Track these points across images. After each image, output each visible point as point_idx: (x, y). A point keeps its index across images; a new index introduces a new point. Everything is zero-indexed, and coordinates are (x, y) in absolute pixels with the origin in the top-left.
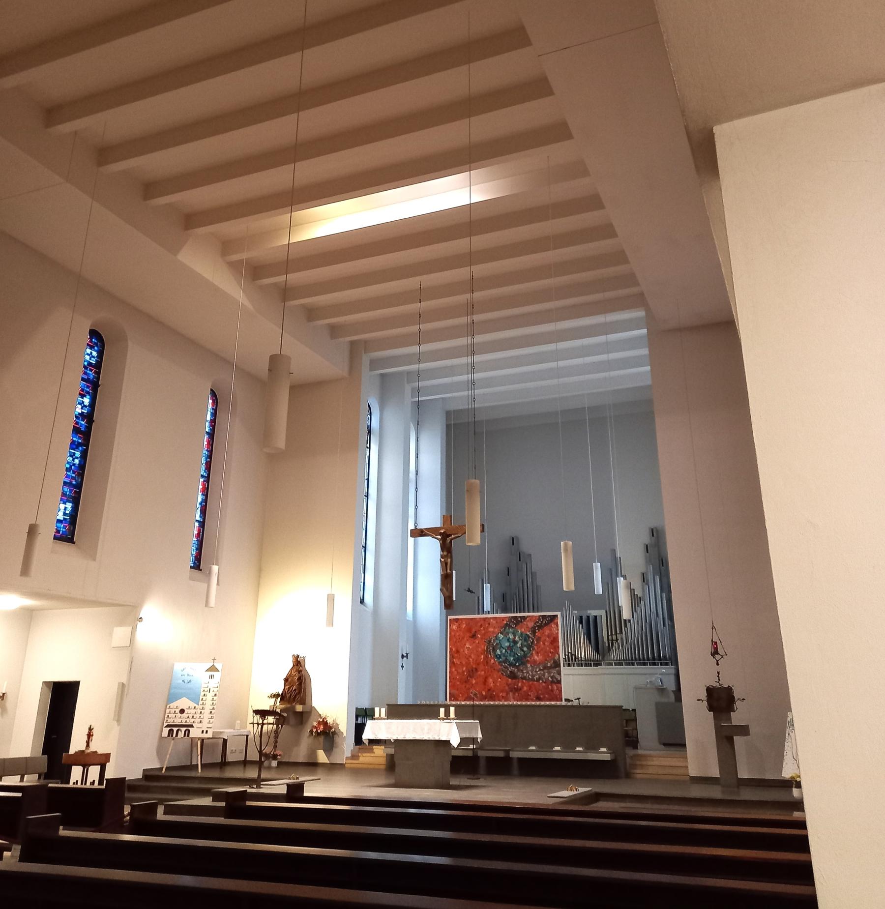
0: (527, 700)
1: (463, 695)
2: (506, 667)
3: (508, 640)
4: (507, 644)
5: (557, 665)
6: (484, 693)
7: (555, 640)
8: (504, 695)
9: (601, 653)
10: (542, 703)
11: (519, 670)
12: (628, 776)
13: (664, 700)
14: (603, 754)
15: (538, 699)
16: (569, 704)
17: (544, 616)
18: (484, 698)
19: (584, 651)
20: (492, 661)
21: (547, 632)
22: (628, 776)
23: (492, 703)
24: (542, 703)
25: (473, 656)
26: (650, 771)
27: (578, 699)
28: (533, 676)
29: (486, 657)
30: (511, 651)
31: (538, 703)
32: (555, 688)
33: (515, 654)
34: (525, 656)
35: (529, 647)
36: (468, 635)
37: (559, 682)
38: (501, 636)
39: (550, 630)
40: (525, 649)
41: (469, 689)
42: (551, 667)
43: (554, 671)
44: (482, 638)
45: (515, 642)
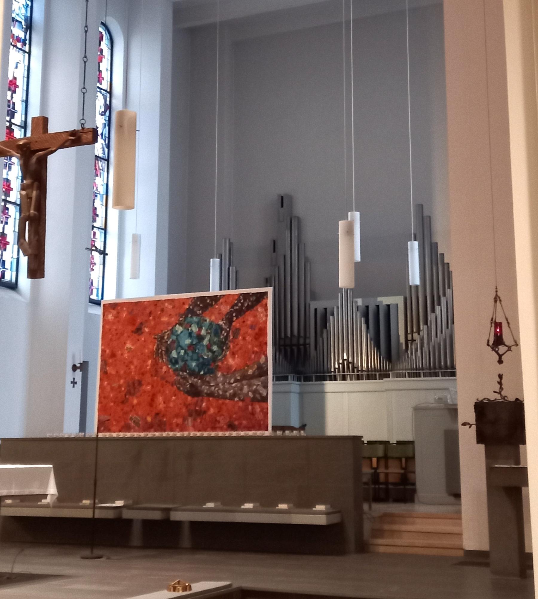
0: (214, 429)
1: (118, 422)
2: (184, 378)
3: (190, 335)
4: (188, 341)
5: (262, 372)
6: (149, 419)
7: (262, 332)
8: (180, 421)
9: (389, 358)
10: (234, 434)
11: (204, 382)
12: (363, 548)
14: (318, 515)
15: (231, 427)
17: (246, 296)
18: (149, 427)
20: (164, 369)
21: (250, 320)
22: (363, 548)
23: (157, 434)
24: (234, 434)
25: (135, 362)
26: (405, 540)
28: (225, 391)
29: (155, 364)
30: (194, 351)
31: (227, 434)
32: (258, 408)
33: (200, 357)
34: (214, 359)
35: (222, 345)
36: (130, 328)
37: (265, 399)
38: (179, 329)
39: (255, 316)
40: (215, 348)
41: (126, 413)
42: (253, 377)
43: (257, 383)
44: (150, 333)
45: (201, 338)
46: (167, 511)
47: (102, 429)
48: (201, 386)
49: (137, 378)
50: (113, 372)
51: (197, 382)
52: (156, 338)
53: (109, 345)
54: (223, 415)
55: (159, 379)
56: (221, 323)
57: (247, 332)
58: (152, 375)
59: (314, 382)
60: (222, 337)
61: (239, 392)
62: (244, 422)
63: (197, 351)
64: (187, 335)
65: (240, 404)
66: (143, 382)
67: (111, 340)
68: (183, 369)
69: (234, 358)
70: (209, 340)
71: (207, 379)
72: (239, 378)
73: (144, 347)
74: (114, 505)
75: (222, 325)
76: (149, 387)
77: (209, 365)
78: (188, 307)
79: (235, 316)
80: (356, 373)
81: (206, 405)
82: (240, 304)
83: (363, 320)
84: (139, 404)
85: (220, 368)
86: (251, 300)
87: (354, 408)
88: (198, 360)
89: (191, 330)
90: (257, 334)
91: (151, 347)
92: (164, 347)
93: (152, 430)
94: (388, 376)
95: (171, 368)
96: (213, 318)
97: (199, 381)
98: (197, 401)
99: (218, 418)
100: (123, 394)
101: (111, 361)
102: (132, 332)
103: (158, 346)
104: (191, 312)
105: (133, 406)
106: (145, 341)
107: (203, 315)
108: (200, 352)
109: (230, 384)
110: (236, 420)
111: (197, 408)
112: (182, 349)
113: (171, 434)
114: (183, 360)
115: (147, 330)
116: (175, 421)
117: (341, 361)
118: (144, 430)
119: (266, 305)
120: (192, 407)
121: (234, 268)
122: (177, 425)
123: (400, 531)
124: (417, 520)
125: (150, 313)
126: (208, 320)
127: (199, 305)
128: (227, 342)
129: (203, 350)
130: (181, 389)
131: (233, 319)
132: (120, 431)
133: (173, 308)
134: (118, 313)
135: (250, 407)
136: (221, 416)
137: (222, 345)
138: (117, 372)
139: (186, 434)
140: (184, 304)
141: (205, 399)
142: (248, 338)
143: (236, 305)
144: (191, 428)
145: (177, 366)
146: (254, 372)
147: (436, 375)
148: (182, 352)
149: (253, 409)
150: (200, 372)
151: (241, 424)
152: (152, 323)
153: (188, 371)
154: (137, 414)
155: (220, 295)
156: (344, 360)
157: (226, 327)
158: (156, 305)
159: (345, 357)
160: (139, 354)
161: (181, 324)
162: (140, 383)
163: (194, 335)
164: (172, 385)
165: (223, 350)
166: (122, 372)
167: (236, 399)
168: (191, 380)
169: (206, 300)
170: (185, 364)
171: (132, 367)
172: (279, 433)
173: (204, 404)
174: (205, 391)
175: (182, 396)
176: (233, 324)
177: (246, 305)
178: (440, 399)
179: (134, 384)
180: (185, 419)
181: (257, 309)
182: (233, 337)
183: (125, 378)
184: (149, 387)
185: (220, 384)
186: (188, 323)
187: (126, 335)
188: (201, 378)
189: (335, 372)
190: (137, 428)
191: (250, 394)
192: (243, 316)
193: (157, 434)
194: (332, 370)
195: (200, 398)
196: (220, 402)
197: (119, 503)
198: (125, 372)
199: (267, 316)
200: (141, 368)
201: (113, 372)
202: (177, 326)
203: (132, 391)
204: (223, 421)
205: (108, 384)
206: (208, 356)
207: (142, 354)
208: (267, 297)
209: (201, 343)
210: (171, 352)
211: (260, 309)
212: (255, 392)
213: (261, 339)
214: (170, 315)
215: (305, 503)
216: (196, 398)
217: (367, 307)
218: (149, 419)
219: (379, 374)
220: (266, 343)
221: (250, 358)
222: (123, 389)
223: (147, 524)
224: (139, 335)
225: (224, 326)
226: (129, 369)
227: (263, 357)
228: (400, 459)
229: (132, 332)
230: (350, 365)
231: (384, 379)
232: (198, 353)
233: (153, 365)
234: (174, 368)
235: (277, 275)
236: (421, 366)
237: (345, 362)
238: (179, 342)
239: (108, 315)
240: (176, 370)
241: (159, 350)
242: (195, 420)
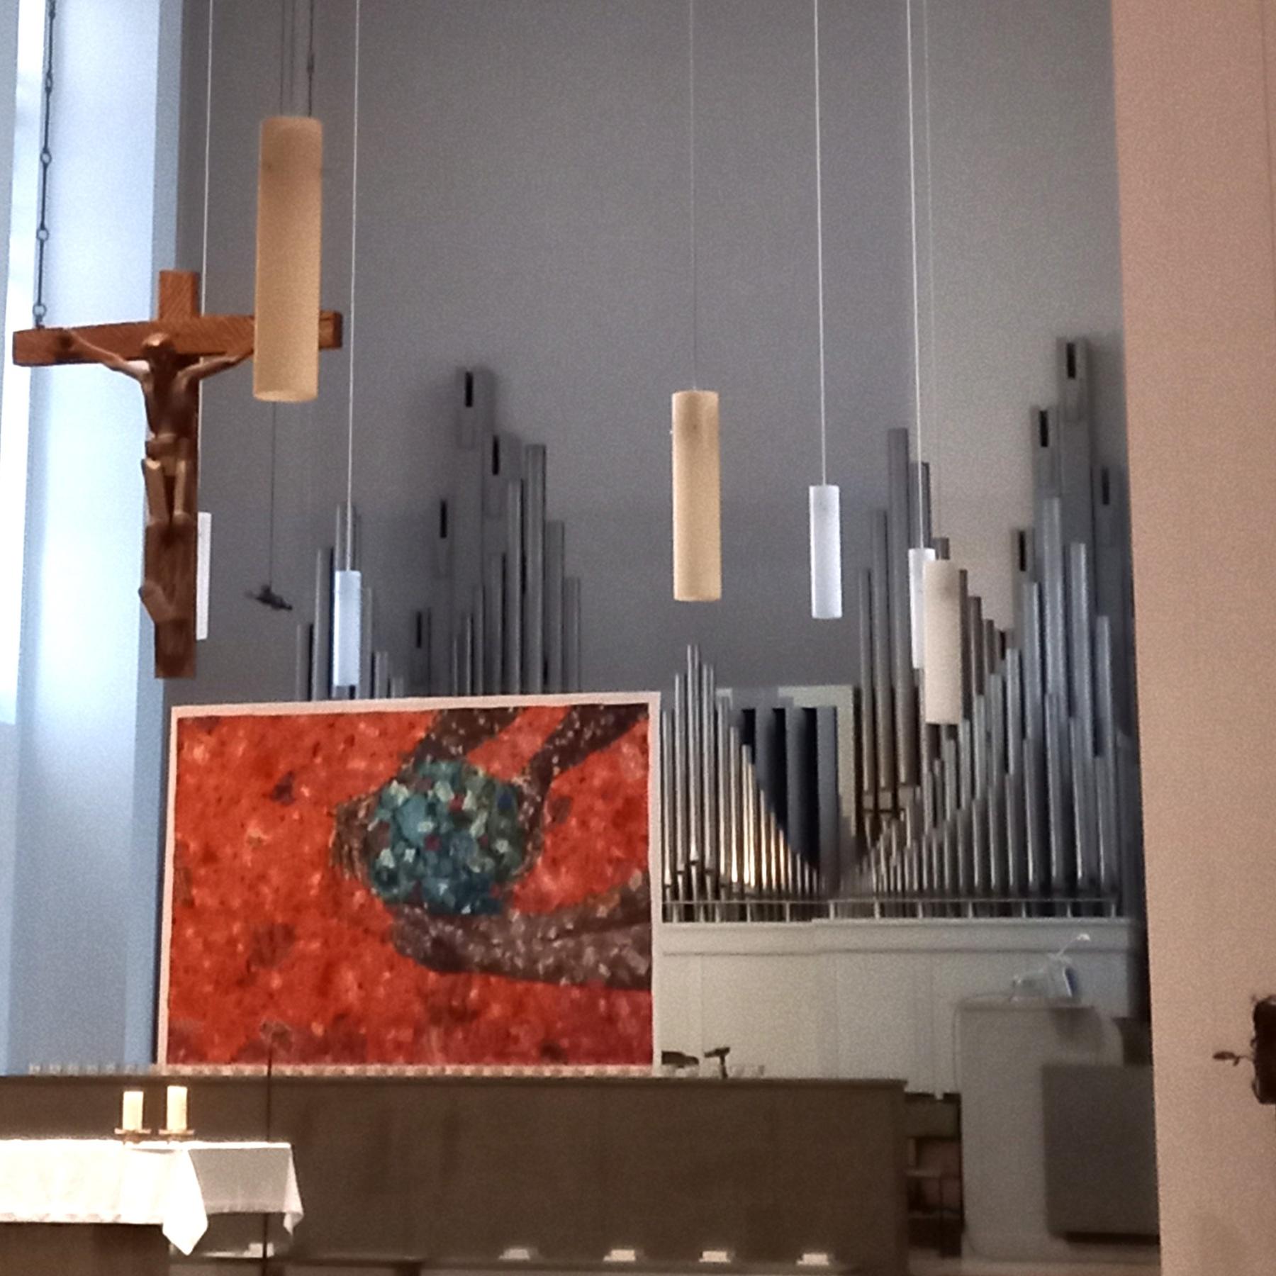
0: (502, 1056)
2: (417, 923)
3: (432, 809)
4: (426, 826)
5: (635, 912)
7: (634, 809)
11: (471, 933)
13: (1075, 1056)
15: (551, 1052)
16: (682, 1073)
17: (588, 712)
19: (754, 859)
20: (359, 896)
25: (275, 875)
27: (721, 1053)
28: (532, 960)
29: (333, 883)
30: (443, 853)
31: (548, 1071)
32: (623, 1006)
33: (458, 869)
34: (501, 874)
35: (523, 838)
36: (257, 785)
37: (644, 983)
38: (400, 793)
39: (614, 767)
40: (503, 846)
44: (316, 802)
45: (461, 819)
48: (465, 945)
49: (280, 919)
51: (453, 934)
54: (528, 1022)
55: (345, 925)
56: (518, 780)
57: (591, 809)
58: (323, 914)
60: (521, 818)
61: (573, 962)
62: (586, 1042)
63: (451, 853)
64: (423, 809)
65: (576, 993)
66: (299, 931)
67: (203, 815)
71: (483, 927)
72: (570, 926)
75: (520, 787)
76: (315, 946)
79: (559, 764)
81: (479, 995)
82: (570, 734)
85: (517, 898)
86: (603, 722)
87: (727, 997)
88: (454, 875)
89: (435, 796)
90: (618, 813)
92: (356, 840)
93: (328, 1058)
94: (822, 912)
95: (378, 895)
96: (496, 766)
97: (460, 932)
99: (514, 1031)
100: (241, 962)
101: (202, 872)
102: (264, 795)
103: (339, 835)
104: (432, 748)
105: (271, 996)
106: (301, 821)
107: (469, 757)
109: (546, 941)
111: (455, 1003)
112: (410, 846)
115: (306, 791)
116: (392, 1034)
117: (681, 867)
119: (644, 738)
122: (399, 1046)
125: (315, 750)
126: (481, 773)
128: (536, 831)
130: (409, 951)
131: (551, 772)
133: (380, 735)
134: (223, 743)
135: (602, 1003)
136: (522, 1023)
137: (523, 838)
138: (222, 903)
140: (412, 726)
142: (596, 824)
143: (561, 734)
144: (439, 1055)
145: (395, 891)
148: (410, 854)
149: (611, 1005)
150: (459, 907)
152: (323, 774)
153: (426, 906)
155: (516, 709)
156: (688, 864)
157: (534, 793)
158: (332, 726)
159: (694, 855)
160: (285, 855)
161: (402, 781)
162: (289, 934)
163: (443, 810)
164: (383, 941)
165: (524, 852)
166: (236, 903)
167: (563, 981)
168: (436, 927)
169: (476, 720)
170: (419, 884)
171: (266, 890)
173: (474, 994)
174: (477, 959)
175: (410, 970)
176: (553, 785)
177: (588, 734)
179: (271, 935)
180: (419, 1032)
181: (619, 748)
182: (554, 819)
183: (246, 920)
184: (315, 946)
185: (519, 943)
186: (424, 777)
187: (245, 802)
188: (465, 923)
191: (603, 969)
192: (580, 765)
195: (462, 977)
196: (520, 987)
198: (246, 904)
199: (646, 767)
200: (290, 895)
202: (395, 783)
204: (525, 1037)
205: (198, 934)
206: (483, 867)
207: (293, 856)
208: (647, 718)
209: (463, 832)
210: (378, 855)
211: (626, 749)
212: (615, 964)
213: (632, 827)
214: (373, 755)
216: (449, 979)
218: (318, 1029)
219: (792, 906)
220: (645, 839)
222: (240, 947)
224: (285, 804)
225: (526, 789)
226: (258, 894)
229: (264, 795)
230: (708, 880)
232: (454, 861)
233: (324, 888)
234: (386, 895)
236: (916, 886)
237: (694, 870)
238: (399, 829)
239: (191, 749)
240: (391, 903)
241: (342, 847)
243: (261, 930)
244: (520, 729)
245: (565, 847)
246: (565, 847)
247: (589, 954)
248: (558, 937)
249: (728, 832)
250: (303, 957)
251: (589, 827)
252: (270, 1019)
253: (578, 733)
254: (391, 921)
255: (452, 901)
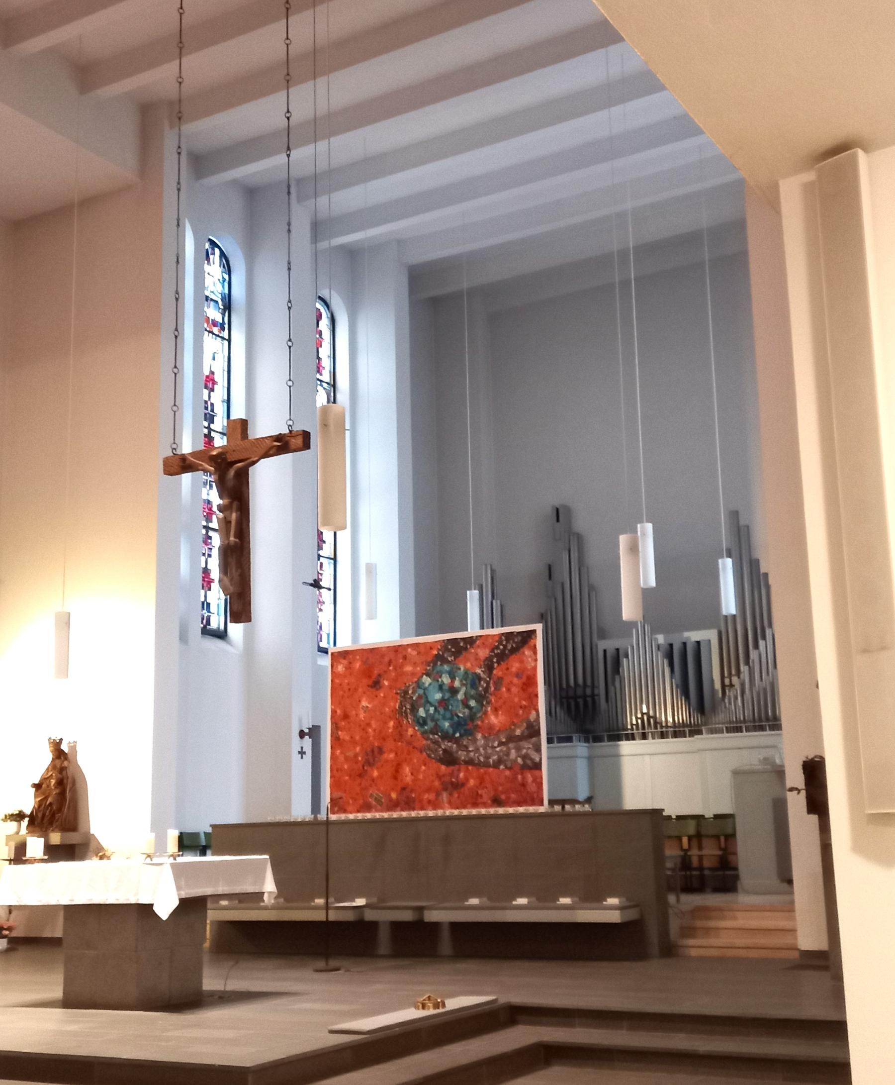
0: (475, 805)
1: (355, 799)
2: (436, 742)
3: (441, 688)
4: (438, 696)
5: (534, 732)
6: (394, 795)
7: (531, 682)
8: (432, 796)
9: (702, 708)
10: (501, 811)
12: (669, 950)
14: (610, 911)
15: (497, 802)
17: (509, 636)
18: (393, 806)
20: (410, 731)
22: (669, 950)
23: (404, 814)
24: (501, 811)
25: (373, 723)
26: (724, 940)
28: (487, 757)
29: (399, 725)
30: (446, 709)
31: (492, 811)
32: (529, 778)
33: (454, 714)
34: (472, 717)
35: (481, 698)
37: (538, 766)
38: (426, 680)
39: (522, 662)
40: (472, 703)
42: (522, 738)
43: (527, 747)
45: (454, 691)
46: (421, 909)
47: (336, 809)
48: (457, 752)
49: (376, 744)
50: (347, 738)
51: (451, 747)
52: (397, 693)
53: (340, 703)
56: (478, 671)
57: (511, 682)
58: (395, 740)
59: (606, 743)
62: (513, 796)
65: (508, 773)
66: (385, 749)
67: (343, 697)
68: (434, 731)
69: (497, 716)
70: (465, 694)
72: (504, 740)
73: (384, 704)
74: (354, 904)
76: (392, 756)
77: (466, 724)
78: (436, 652)
80: (659, 730)
82: (501, 647)
83: (666, 662)
84: (381, 776)
85: (480, 728)
88: (451, 719)
90: (524, 684)
91: (392, 704)
92: (409, 704)
93: (399, 808)
94: (700, 732)
96: (469, 665)
98: (453, 771)
99: (480, 792)
100: (360, 765)
103: (401, 702)
104: (440, 658)
105: (373, 780)
106: (384, 697)
108: (454, 708)
109: (493, 747)
110: (502, 793)
112: (432, 705)
113: (422, 813)
114: (433, 720)
115: (386, 683)
116: (426, 796)
117: (639, 716)
118: (388, 809)
119: (535, 646)
120: (447, 779)
121: (499, 602)
122: (429, 802)
123: (718, 929)
124: (738, 914)
125: (390, 663)
126: (462, 669)
127: (450, 650)
129: (457, 706)
132: (358, 811)
134: (350, 663)
135: (519, 777)
137: (481, 698)
139: (440, 812)
140: (431, 648)
141: (463, 767)
142: (514, 690)
143: (497, 647)
144: (447, 805)
146: (522, 733)
147: (762, 728)
148: (432, 710)
149: (524, 778)
150: (454, 733)
151: (508, 798)
152: (393, 674)
154: (379, 790)
156: (643, 714)
159: (645, 710)
160: (378, 713)
161: (428, 675)
162: (381, 751)
163: (446, 688)
164: (421, 752)
165: (482, 705)
166: (357, 738)
167: (502, 767)
170: (436, 725)
172: (558, 808)
173: (462, 775)
176: (495, 672)
177: (509, 647)
178: (765, 759)
179: (373, 751)
180: (438, 794)
181: (524, 653)
183: (362, 745)
184: (392, 756)
185: (481, 749)
186: (438, 672)
187: (360, 690)
188: (457, 741)
189: (632, 729)
190: (379, 807)
191: (520, 760)
193: (404, 814)
194: (629, 727)
195: (457, 766)
197: (360, 902)
198: (361, 737)
199: (536, 660)
200: (380, 732)
201: (347, 738)
203: (371, 760)
204: (486, 794)
205: (341, 753)
206: (464, 713)
212: (525, 757)
213: (530, 690)
214: (415, 663)
215: (594, 897)
216: (452, 768)
217: (671, 645)
218: (394, 795)
220: (537, 696)
221: (517, 715)
223: (396, 926)
224: (377, 690)
225: (482, 675)
227: (534, 713)
228: (717, 837)
230: (652, 720)
231: (696, 736)
232: (451, 711)
233: (395, 728)
234: (422, 730)
235: (553, 610)
240: (424, 733)
242: (451, 794)
243: (369, 750)
244: (478, 646)
245: (501, 702)
246: (501, 702)
247: (513, 753)
248: (499, 745)
249: (659, 699)
250: (387, 761)
251: (512, 693)
252: (373, 791)
253: (505, 646)
254: (424, 742)
255: (451, 731)
